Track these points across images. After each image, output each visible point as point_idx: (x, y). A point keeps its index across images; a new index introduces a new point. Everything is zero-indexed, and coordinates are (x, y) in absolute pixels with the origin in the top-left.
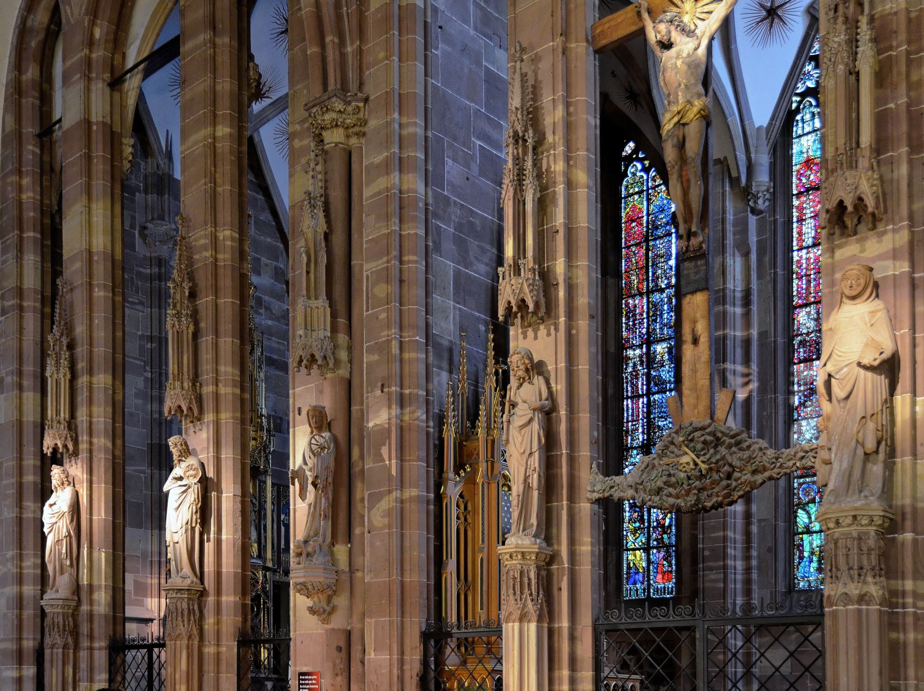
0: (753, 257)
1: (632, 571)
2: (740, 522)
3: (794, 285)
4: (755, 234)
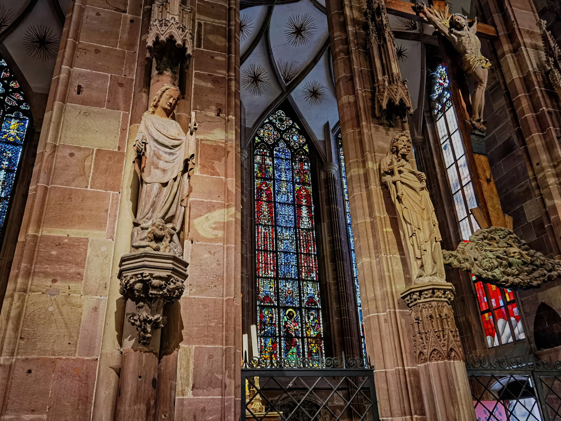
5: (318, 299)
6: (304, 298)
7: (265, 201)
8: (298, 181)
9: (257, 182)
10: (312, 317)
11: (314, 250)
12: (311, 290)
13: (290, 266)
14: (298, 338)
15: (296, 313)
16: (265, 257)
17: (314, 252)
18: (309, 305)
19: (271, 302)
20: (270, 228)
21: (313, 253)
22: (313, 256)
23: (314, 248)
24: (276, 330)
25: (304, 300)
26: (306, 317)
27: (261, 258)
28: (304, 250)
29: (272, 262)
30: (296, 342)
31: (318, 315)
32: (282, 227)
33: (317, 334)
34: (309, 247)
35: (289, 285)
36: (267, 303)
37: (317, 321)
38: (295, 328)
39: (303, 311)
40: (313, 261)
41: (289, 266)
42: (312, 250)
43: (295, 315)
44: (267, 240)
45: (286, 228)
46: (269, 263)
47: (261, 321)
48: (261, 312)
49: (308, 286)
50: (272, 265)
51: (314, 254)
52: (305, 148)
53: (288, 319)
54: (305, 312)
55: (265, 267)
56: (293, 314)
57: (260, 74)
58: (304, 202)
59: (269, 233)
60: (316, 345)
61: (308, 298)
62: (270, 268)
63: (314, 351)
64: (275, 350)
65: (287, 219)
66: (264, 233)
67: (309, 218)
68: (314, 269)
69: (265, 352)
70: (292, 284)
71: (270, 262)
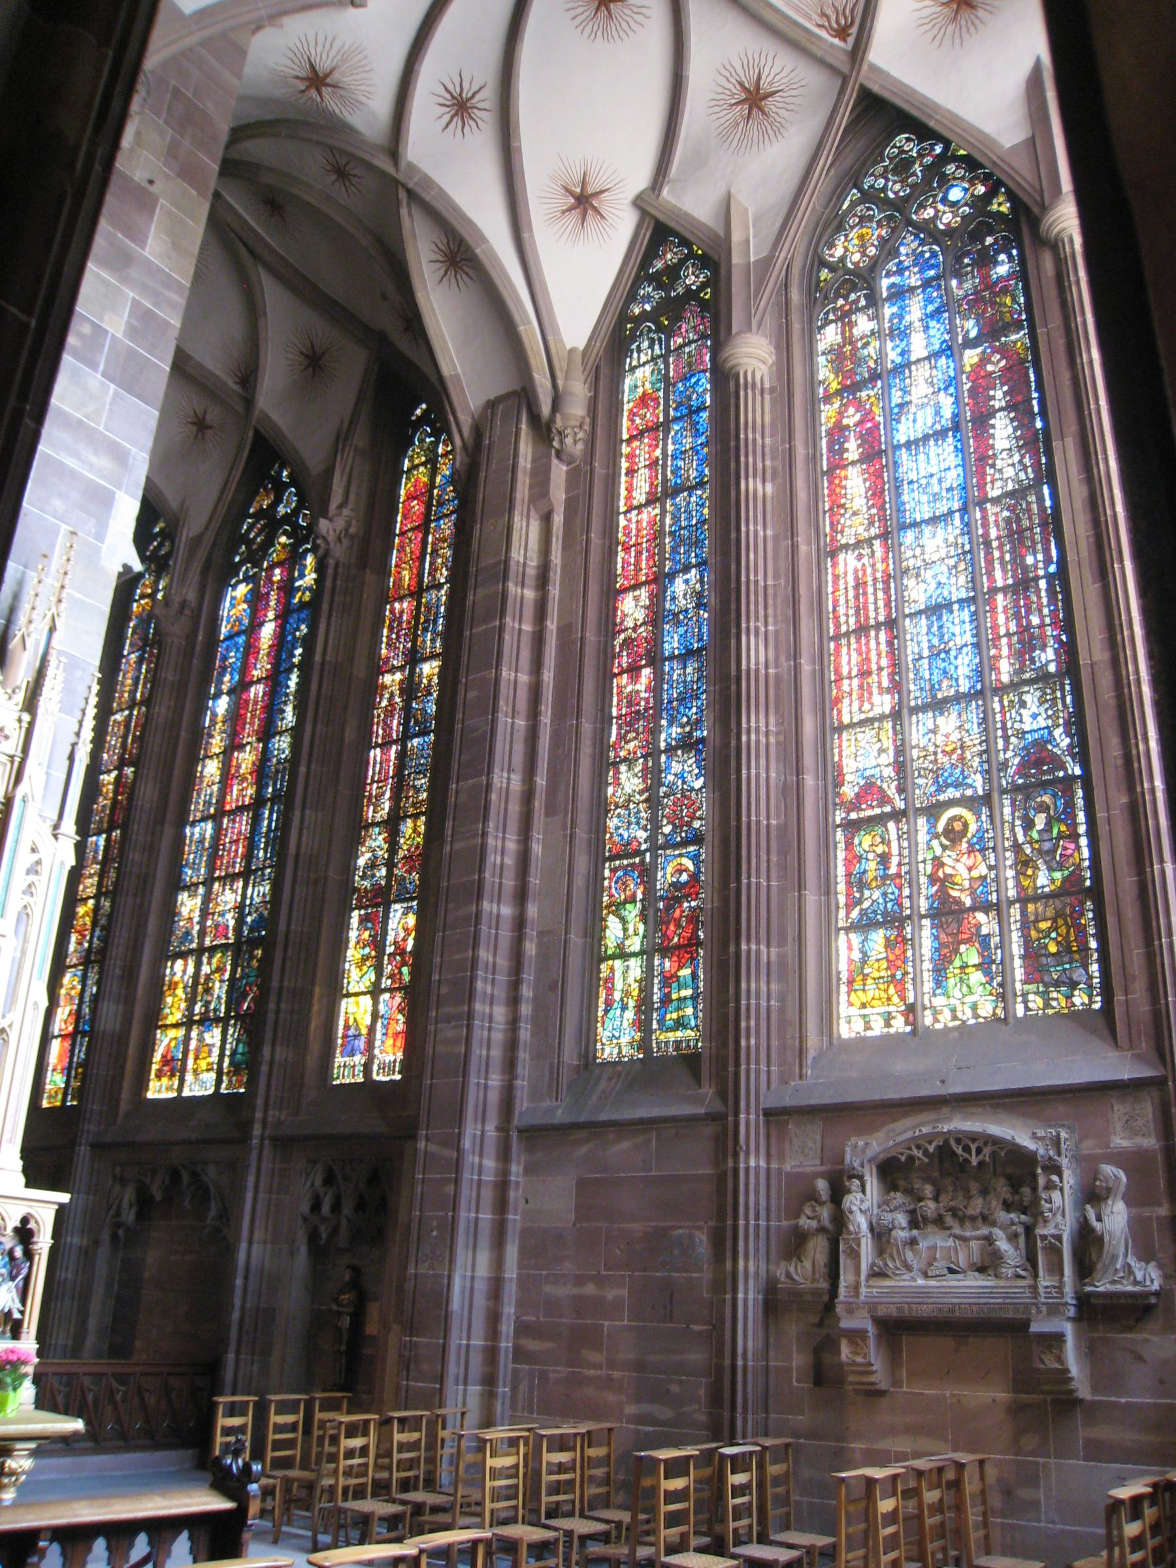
0: (558, 519)
1: (351, 1032)
2: (506, 934)
3: (619, 560)
4: (563, 488)
5: (1068, 740)
6: (1010, 754)
7: (853, 463)
8: (973, 334)
9: (828, 413)
10: (1040, 821)
11: (1048, 561)
12: (1035, 716)
13: (953, 653)
14: (986, 907)
15: (978, 818)
16: (860, 654)
17: (1046, 568)
18: (1026, 776)
19: (884, 799)
20: (877, 544)
21: (1041, 573)
22: (1043, 584)
23: (1047, 551)
24: (900, 895)
25: (1007, 760)
26: (1018, 822)
27: (848, 660)
28: (1004, 571)
29: (884, 662)
30: (978, 926)
31: (1070, 805)
32: (915, 524)
33: (1065, 880)
34: (1023, 558)
35: (948, 723)
36: (872, 807)
37: (1063, 828)
38: (975, 873)
39: (1007, 802)
40: (1045, 601)
41: (947, 652)
42: (1037, 562)
43: (973, 828)
44: (865, 594)
45: (934, 520)
46: (874, 667)
47: (848, 875)
48: (849, 845)
49: (1023, 704)
50: (885, 673)
51: (1049, 577)
52: (995, 207)
53: (944, 848)
54: (1013, 804)
55: (861, 687)
56: (966, 825)
57: (759, 78)
58: (999, 397)
59: (873, 566)
60: (1060, 922)
61: (1024, 748)
62: (880, 683)
63: (1053, 948)
64: (898, 968)
65: (936, 489)
66: (856, 571)
67: (1019, 448)
68: (1049, 631)
69: (864, 980)
70: (960, 715)
71: (878, 663)
